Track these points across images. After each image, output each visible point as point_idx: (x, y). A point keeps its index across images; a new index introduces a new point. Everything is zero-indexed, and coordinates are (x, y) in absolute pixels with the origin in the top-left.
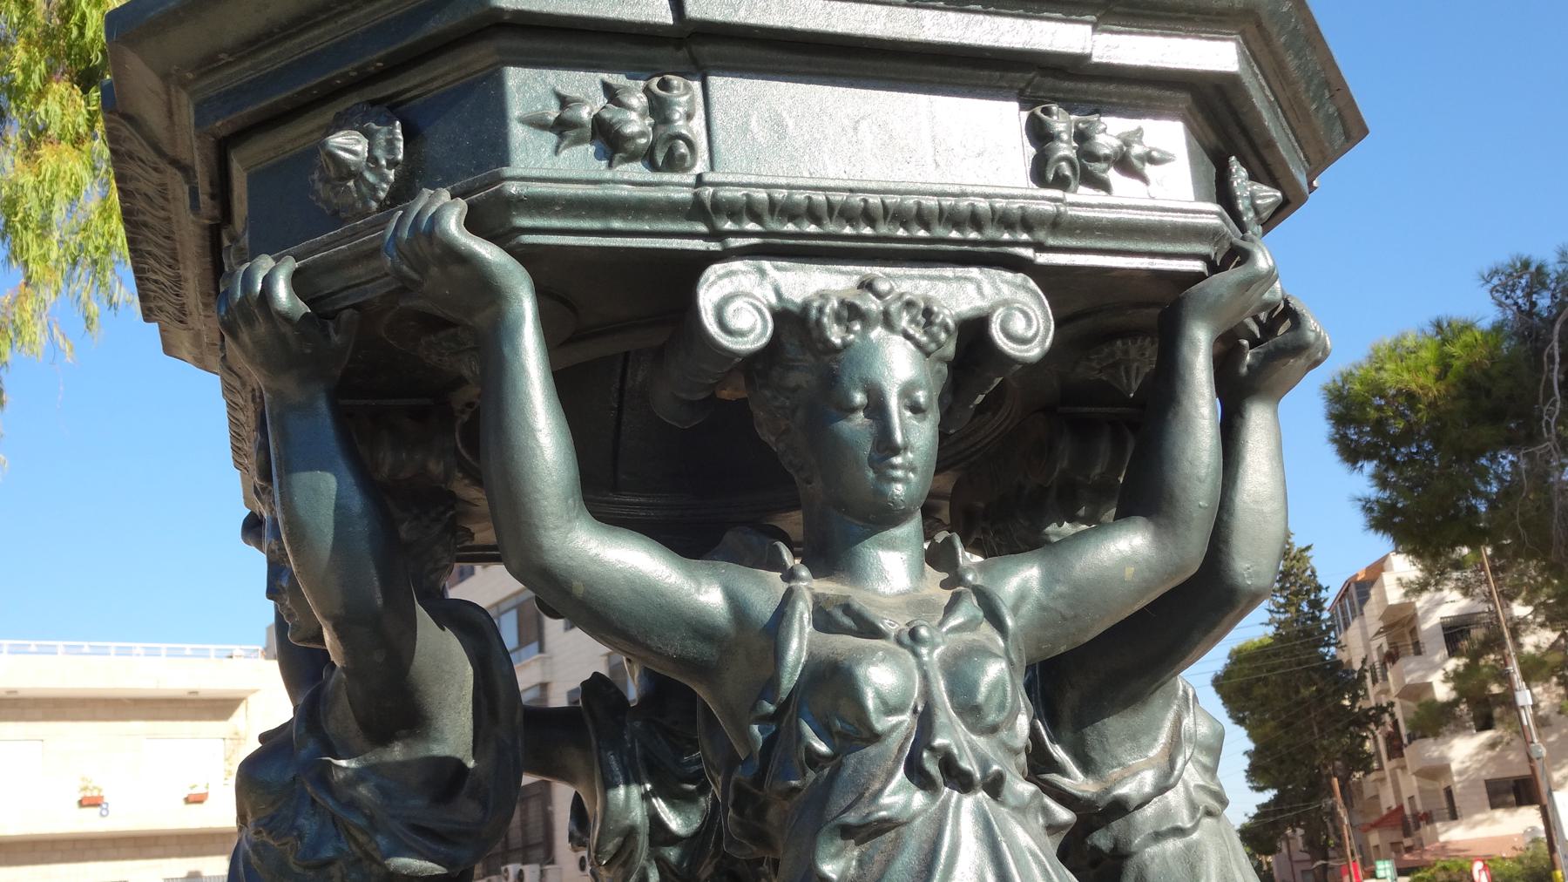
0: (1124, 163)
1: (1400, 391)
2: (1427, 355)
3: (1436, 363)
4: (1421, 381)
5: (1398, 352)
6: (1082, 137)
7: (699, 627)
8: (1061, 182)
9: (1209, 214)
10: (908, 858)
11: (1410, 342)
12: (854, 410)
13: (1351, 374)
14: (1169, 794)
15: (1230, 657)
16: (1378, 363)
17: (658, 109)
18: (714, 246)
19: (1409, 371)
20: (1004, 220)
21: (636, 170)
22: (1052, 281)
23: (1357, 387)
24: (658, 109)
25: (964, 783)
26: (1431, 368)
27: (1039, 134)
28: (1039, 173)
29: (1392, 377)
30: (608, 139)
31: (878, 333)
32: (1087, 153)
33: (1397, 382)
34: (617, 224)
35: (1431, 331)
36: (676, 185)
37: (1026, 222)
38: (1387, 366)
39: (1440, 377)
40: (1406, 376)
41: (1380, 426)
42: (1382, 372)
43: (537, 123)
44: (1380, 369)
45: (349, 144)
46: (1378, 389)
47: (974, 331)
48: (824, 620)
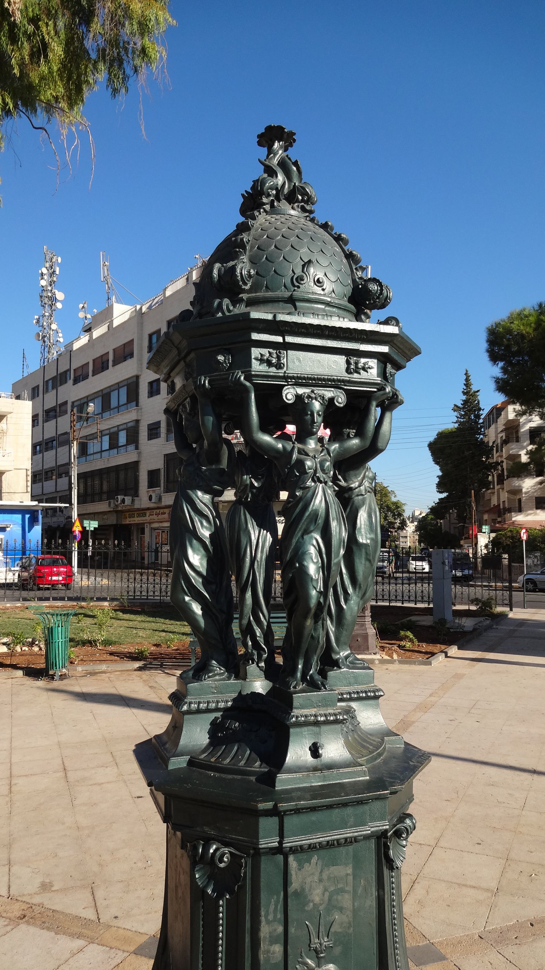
0: (364, 369)
1: (518, 333)
2: (532, 319)
3: (535, 323)
4: (528, 330)
5: (521, 316)
6: (356, 363)
7: (277, 451)
8: (351, 373)
9: (379, 380)
10: (310, 494)
11: (526, 313)
12: (308, 415)
13: (500, 324)
14: (361, 487)
15: (437, 435)
16: (511, 319)
17: (278, 358)
18: (286, 384)
19: (523, 325)
20: (339, 381)
21: (273, 369)
22: (347, 392)
23: (501, 330)
24: (278, 358)
25: (321, 482)
26: (533, 325)
27: (348, 363)
28: (348, 370)
29: (516, 326)
30: (269, 364)
31: (314, 401)
32: (357, 367)
33: (518, 330)
34: (270, 379)
35: (537, 308)
36: (281, 373)
37: (343, 381)
38: (515, 322)
39: (535, 330)
40: (522, 327)
41: (508, 347)
42: (512, 325)
43: (256, 359)
44: (512, 323)
45: (221, 358)
46: (509, 331)
47: (331, 400)
48: (300, 451)
